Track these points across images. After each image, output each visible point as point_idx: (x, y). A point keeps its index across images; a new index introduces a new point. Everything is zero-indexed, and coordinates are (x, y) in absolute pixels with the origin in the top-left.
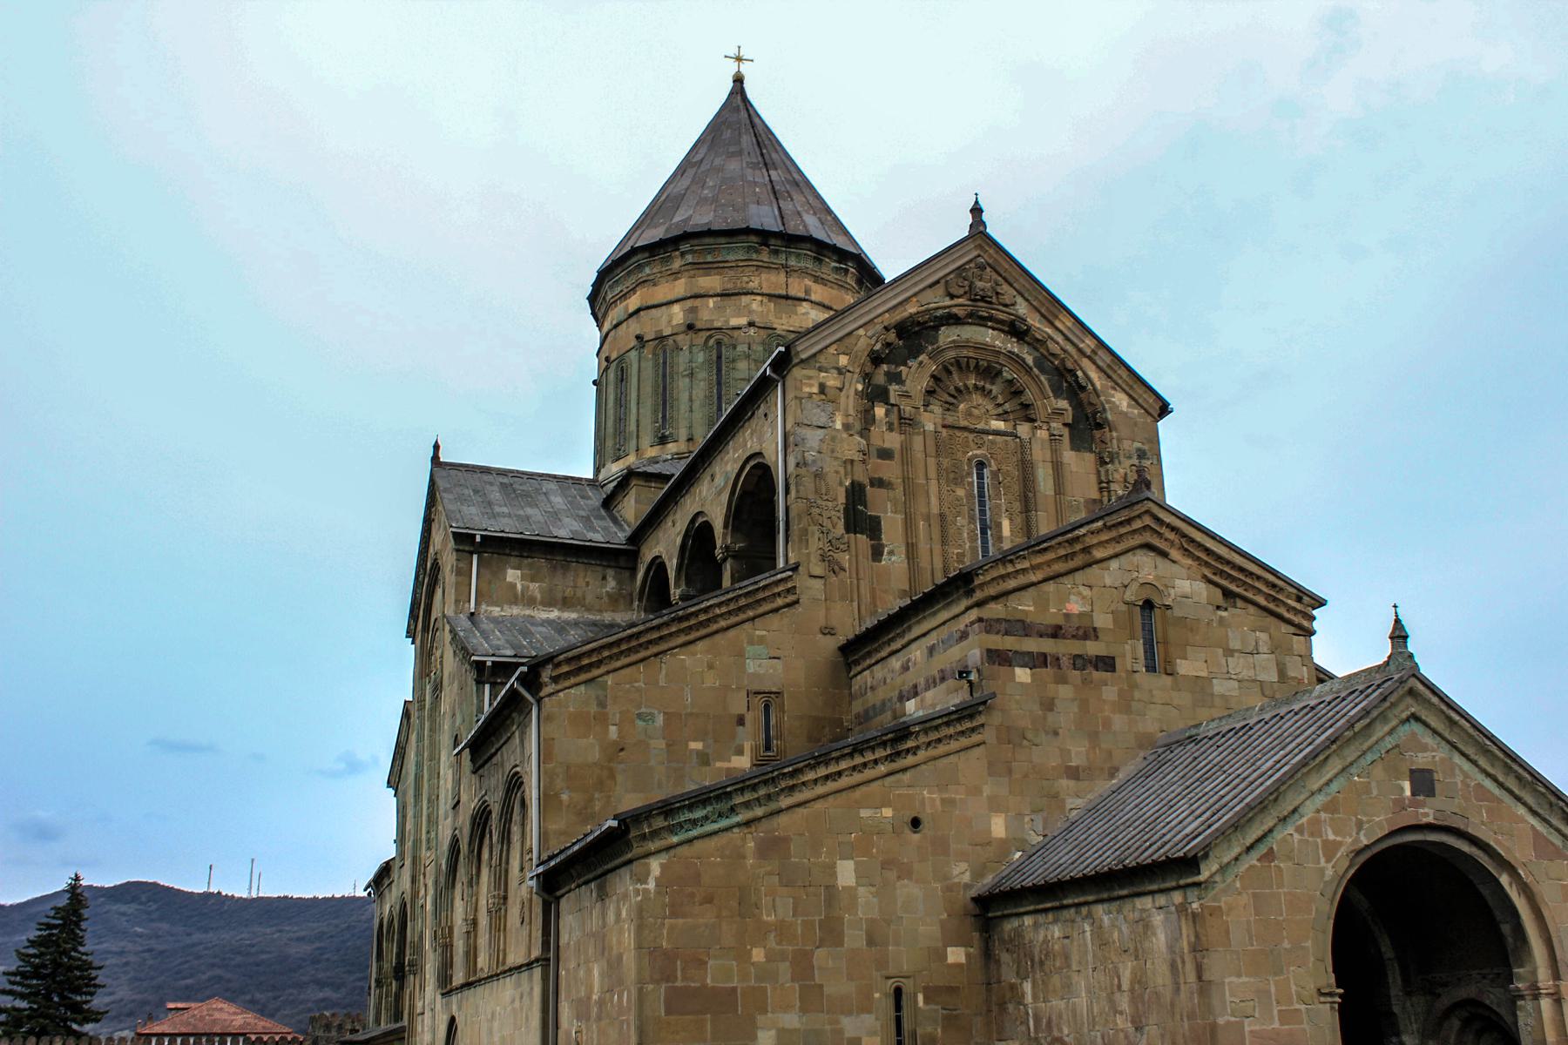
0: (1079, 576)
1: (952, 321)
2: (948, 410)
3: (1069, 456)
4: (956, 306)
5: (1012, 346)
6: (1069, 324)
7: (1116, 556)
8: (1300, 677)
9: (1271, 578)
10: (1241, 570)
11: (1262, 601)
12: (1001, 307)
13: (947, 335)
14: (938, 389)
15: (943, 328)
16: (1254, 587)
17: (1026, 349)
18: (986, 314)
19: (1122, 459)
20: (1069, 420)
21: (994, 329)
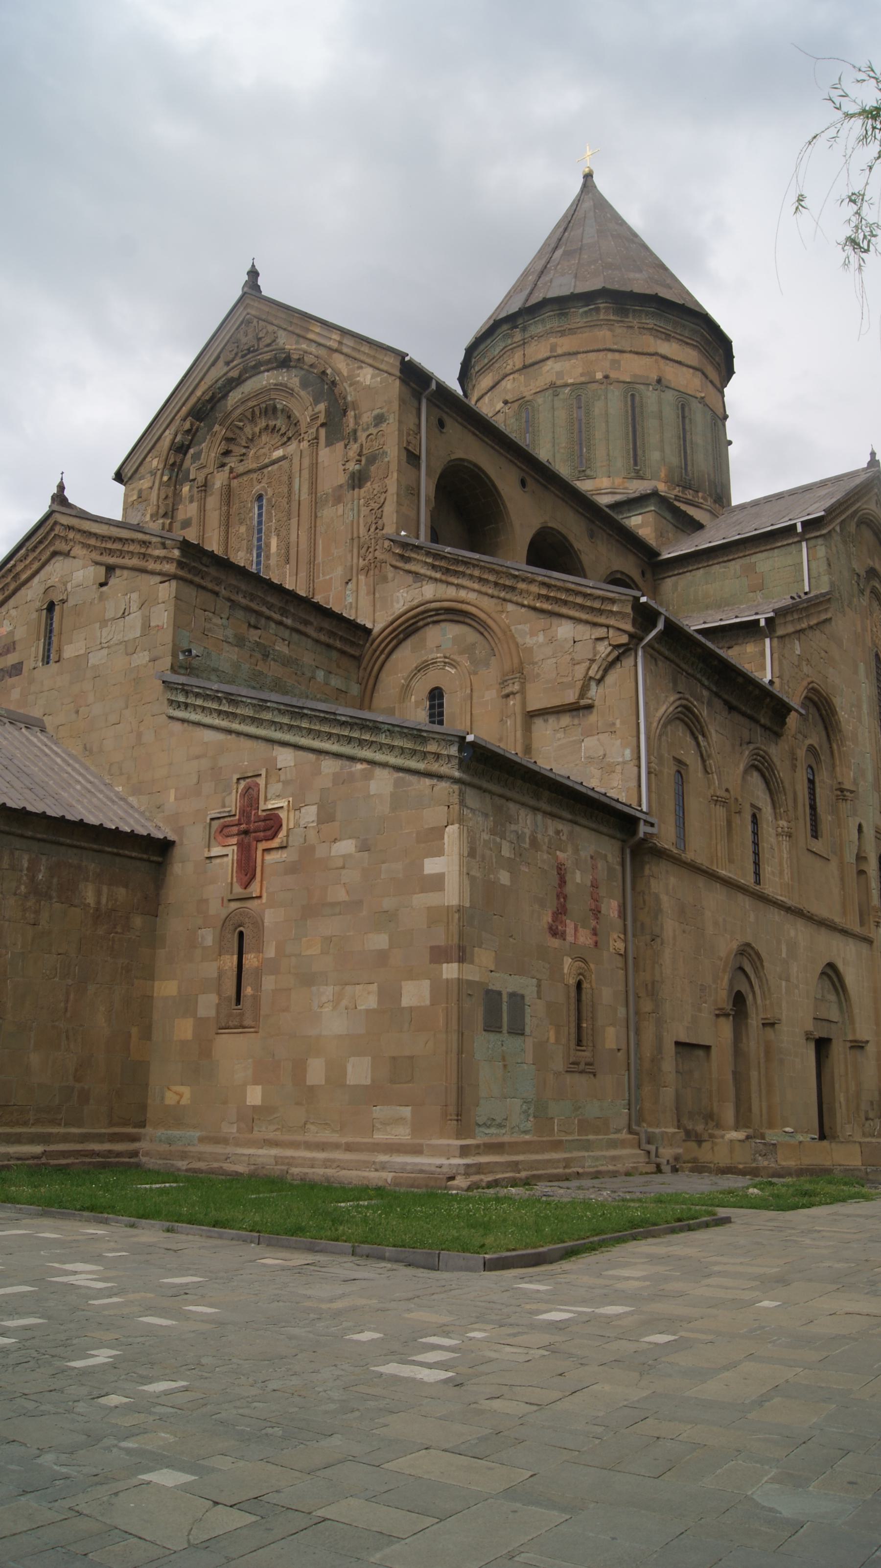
0: (12, 602)
1: (234, 384)
2: (242, 461)
3: (324, 453)
4: (230, 370)
5: (282, 377)
6: (318, 330)
7: (37, 572)
8: (160, 624)
9: (140, 536)
10: (120, 539)
11: (135, 562)
12: (266, 349)
13: (234, 397)
14: (232, 447)
15: (231, 394)
16: (128, 552)
17: (294, 372)
18: (254, 363)
19: (359, 433)
20: (322, 419)
21: (268, 371)
